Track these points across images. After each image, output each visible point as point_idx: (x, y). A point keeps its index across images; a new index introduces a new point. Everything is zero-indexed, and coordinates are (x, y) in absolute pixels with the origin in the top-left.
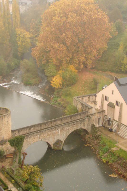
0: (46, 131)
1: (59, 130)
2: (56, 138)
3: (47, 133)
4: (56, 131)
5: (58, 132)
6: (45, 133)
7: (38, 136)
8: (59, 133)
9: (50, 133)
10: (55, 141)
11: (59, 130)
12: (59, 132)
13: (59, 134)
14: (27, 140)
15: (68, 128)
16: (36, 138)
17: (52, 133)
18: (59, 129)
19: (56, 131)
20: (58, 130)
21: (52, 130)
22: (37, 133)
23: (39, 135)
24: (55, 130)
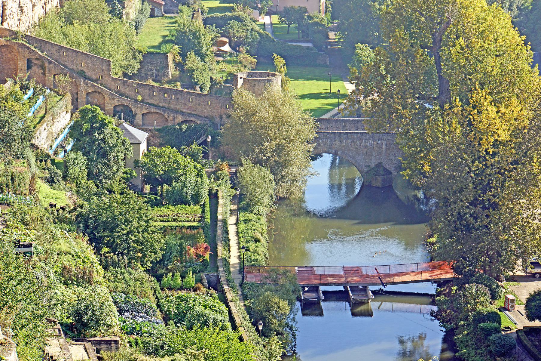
0: (349, 135)
1: (384, 142)
2: (373, 158)
3: (350, 141)
4: (375, 143)
5: (380, 148)
6: (345, 139)
7: (329, 140)
8: (382, 148)
9: (358, 143)
10: (373, 165)
12: (384, 147)
13: (384, 152)
16: (322, 145)
17: (364, 143)
18: (383, 140)
20: (378, 140)
21: (364, 137)
22: (325, 134)
23: (331, 141)
24: (372, 139)
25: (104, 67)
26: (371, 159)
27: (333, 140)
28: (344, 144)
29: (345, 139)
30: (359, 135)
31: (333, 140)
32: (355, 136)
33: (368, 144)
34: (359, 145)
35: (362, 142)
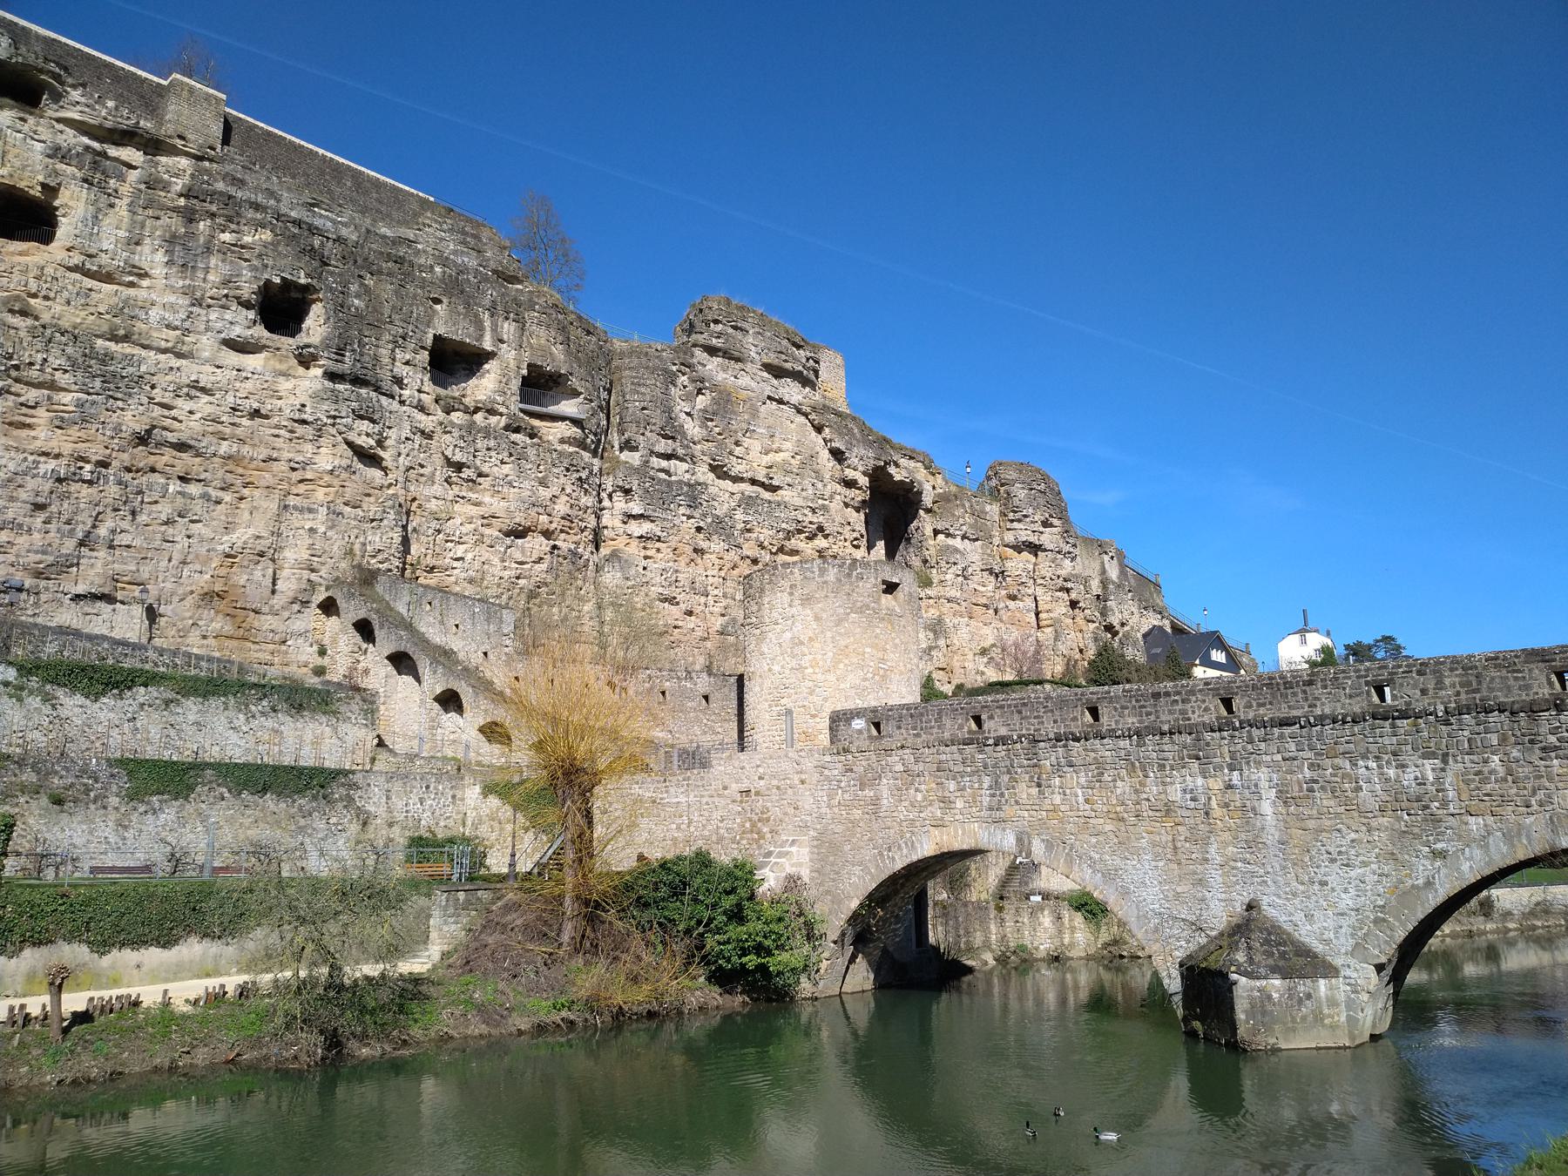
2: (1216, 877)
4: (1216, 784)
5: (1248, 812)
6: (1058, 768)
11: (1262, 776)
12: (1267, 807)
13: (1272, 835)
14: (876, 801)
15: (1408, 778)
16: (959, 804)
17: (1152, 789)
18: (1258, 764)
19: (1216, 784)
24: (1195, 765)
25: (491, 626)
26: (1201, 882)
27: (1006, 778)
28: (1057, 799)
29: (1058, 768)
30: (1122, 743)
31: (1006, 778)
32: (1104, 750)
33: (1175, 793)
34: (1130, 799)
35: (1142, 784)
